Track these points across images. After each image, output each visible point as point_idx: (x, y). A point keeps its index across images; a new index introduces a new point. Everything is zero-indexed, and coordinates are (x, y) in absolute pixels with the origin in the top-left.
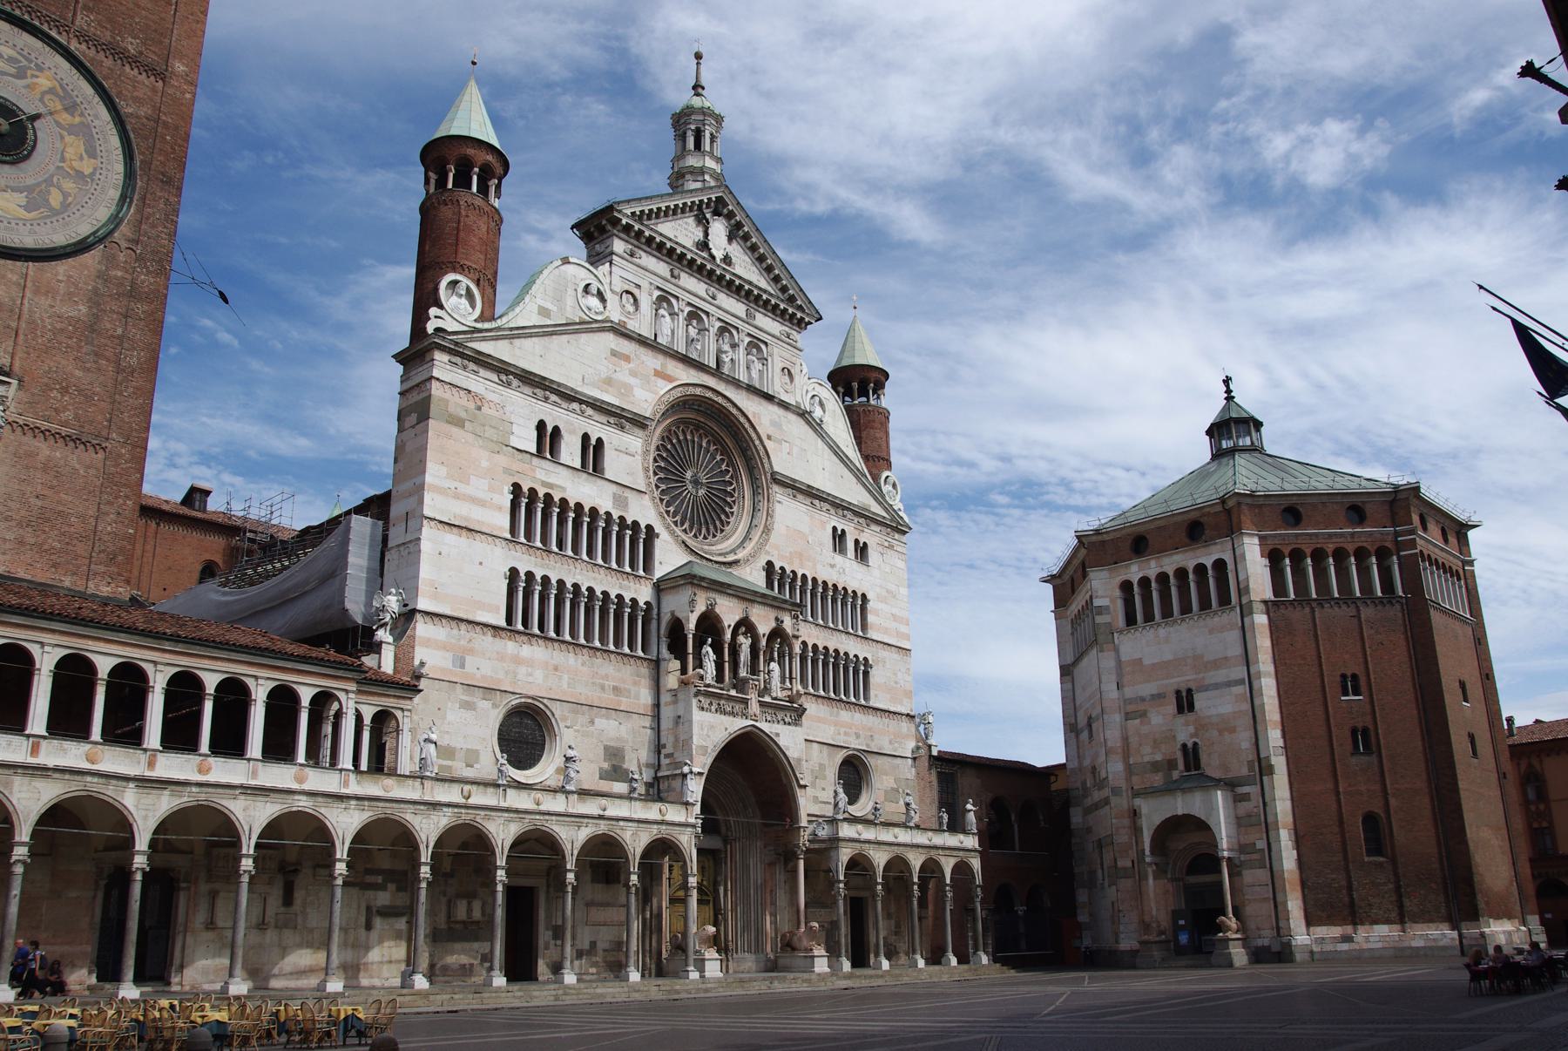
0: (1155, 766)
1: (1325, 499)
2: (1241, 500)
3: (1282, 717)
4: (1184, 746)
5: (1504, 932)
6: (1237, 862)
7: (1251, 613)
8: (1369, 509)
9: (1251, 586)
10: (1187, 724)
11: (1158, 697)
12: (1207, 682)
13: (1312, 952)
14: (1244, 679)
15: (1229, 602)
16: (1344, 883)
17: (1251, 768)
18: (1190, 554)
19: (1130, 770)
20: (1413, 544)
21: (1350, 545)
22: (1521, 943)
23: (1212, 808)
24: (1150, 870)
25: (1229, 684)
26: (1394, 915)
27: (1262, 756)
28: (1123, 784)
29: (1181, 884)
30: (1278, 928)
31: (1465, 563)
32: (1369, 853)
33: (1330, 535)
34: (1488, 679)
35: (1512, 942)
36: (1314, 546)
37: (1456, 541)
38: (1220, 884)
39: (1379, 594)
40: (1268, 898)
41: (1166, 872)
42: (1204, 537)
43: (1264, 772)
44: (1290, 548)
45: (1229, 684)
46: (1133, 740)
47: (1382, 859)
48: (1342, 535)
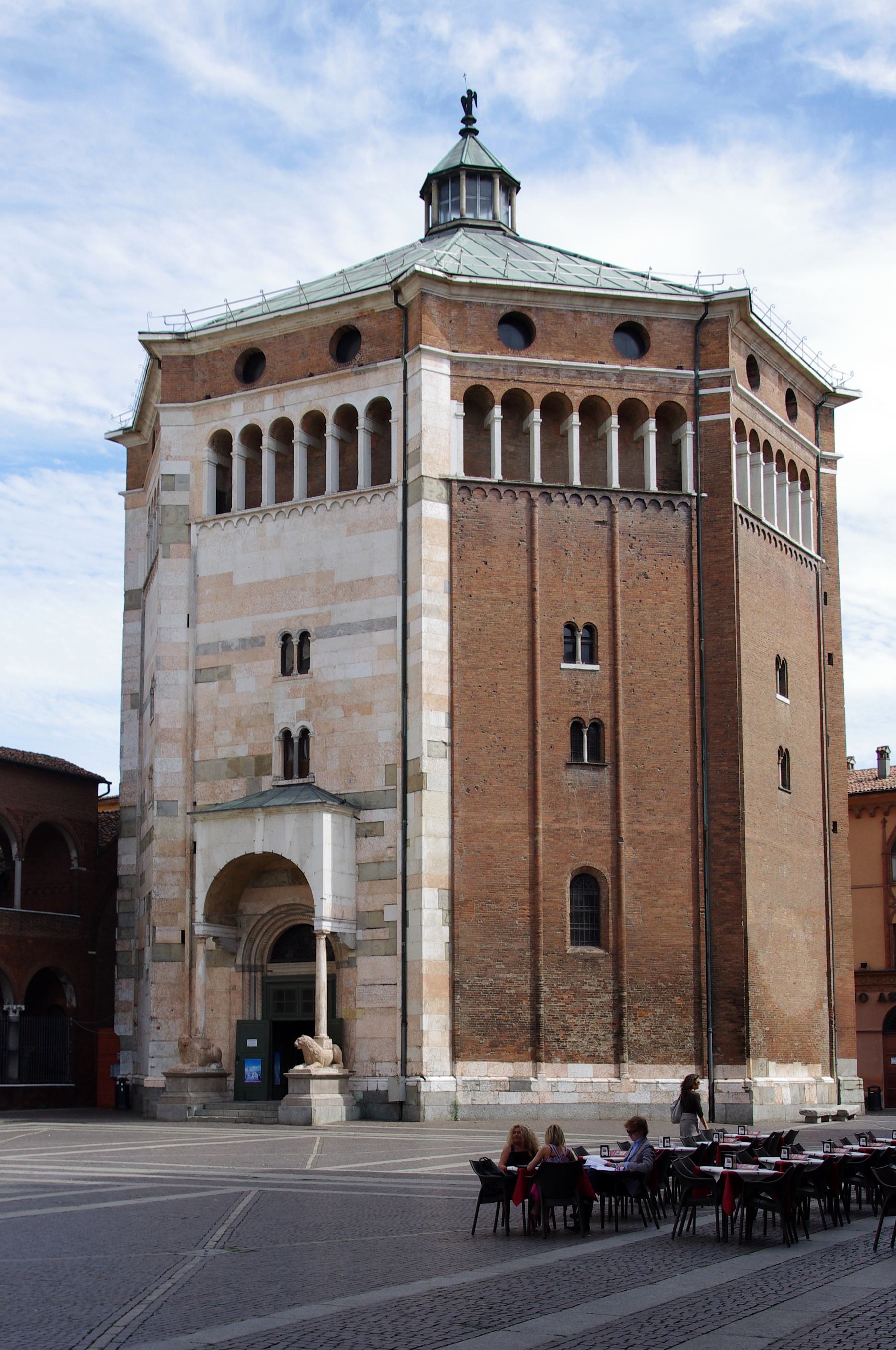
0: (235, 767)
1: (579, 304)
2: (428, 288)
3: (452, 691)
4: (287, 733)
5: (792, 1084)
6: (349, 943)
7: (419, 499)
8: (657, 333)
9: (424, 449)
10: (293, 694)
11: (255, 643)
12: (334, 621)
13: (455, 1105)
14: (395, 618)
15: (386, 477)
16: (526, 989)
17: (390, 780)
18: (332, 387)
19: (192, 769)
20: (723, 403)
21: (614, 393)
22: (821, 1103)
23: (312, 844)
24: (200, 949)
25: (371, 626)
26: (606, 1047)
27: (410, 757)
28: (178, 795)
29: (259, 974)
30: (404, 1061)
31: (820, 460)
32: (578, 938)
33: (581, 373)
34: (831, 662)
35: (803, 1102)
36: (549, 390)
37: (811, 421)
38: (311, 979)
39: (653, 487)
40: (395, 1008)
41: (234, 954)
42: (358, 357)
43: (409, 788)
44: (505, 388)
45: (371, 626)
46: (204, 719)
47: (596, 951)
48: (602, 374)
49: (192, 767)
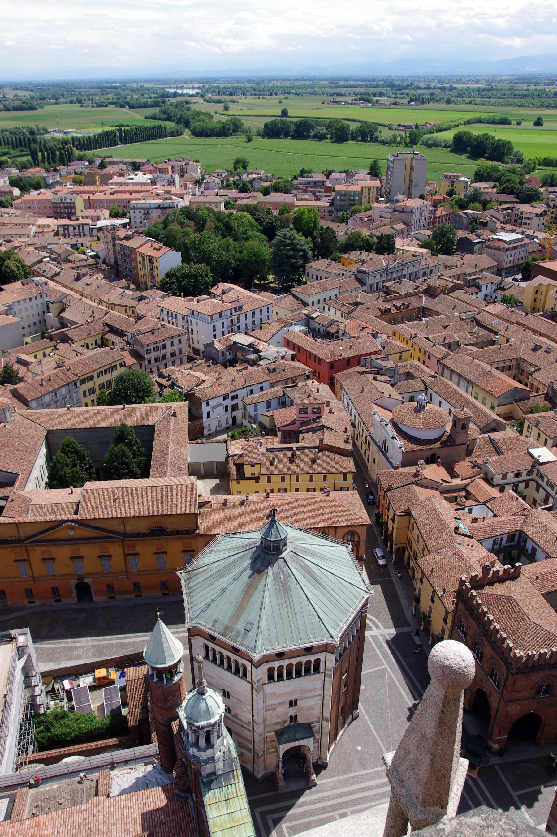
0: (277, 723)
11: (282, 703)
25: (314, 696)
45: (314, 696)
49: (265, 726)
